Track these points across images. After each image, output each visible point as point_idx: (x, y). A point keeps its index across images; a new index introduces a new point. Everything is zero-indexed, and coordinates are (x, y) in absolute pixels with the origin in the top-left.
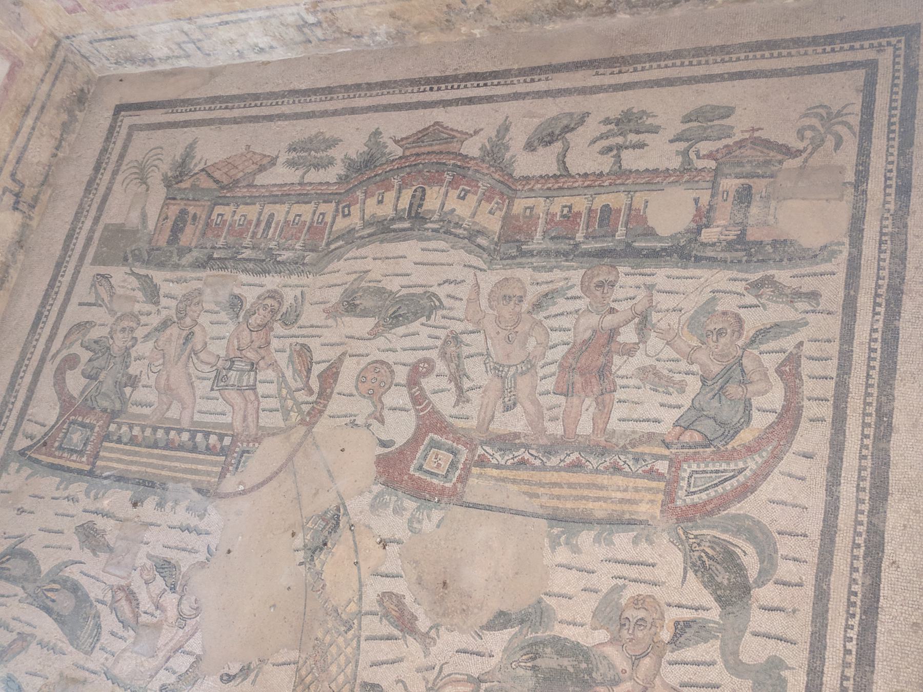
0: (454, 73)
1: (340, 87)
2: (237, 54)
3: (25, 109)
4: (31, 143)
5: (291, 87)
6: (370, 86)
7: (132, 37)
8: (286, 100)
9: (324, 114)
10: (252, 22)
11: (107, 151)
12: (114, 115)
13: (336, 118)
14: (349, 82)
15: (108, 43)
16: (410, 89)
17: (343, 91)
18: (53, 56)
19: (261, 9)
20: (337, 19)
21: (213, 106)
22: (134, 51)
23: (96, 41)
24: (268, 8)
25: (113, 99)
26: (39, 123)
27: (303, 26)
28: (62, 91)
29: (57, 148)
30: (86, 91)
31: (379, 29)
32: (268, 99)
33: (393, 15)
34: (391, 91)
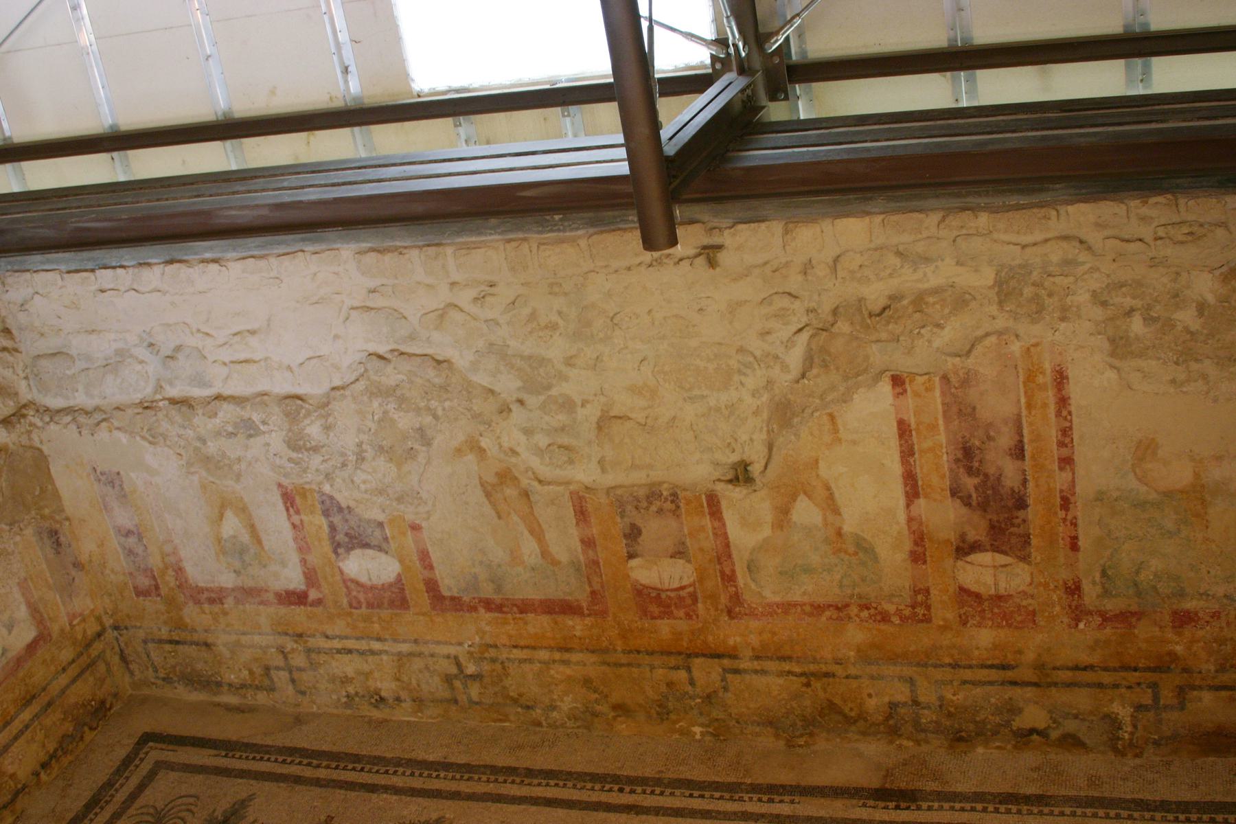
0: (657, 776)
1: (485, 766)
2: (344, 700)
3: (28, 697)
4: (16, 744)
5: (413, 755)
6: (530, 773)
7: (207, 645)
8: (401, 770)
9: (456, 796)
10: (385, 657)
11: (112, 786)
12: (138, 743)
13: (470, 803)
14: (501, 762)
15: (168, 647)
16: (589, 785)
17: (488, 772)
18: (88, 645)
19: (404, 641)
20: (507, 675)
21: (289, 759)
22: (199, 666)
23: (153, 641)
24: (416, 641)
25: (144, 723)
26: (36, 722)
27: (456, 676)
28: (83, 691)
29: (44, 765)
30: (108, 706)
31: (562, 701)
32: (374, 764)
33: (587, 682)
34: (561, 783)
